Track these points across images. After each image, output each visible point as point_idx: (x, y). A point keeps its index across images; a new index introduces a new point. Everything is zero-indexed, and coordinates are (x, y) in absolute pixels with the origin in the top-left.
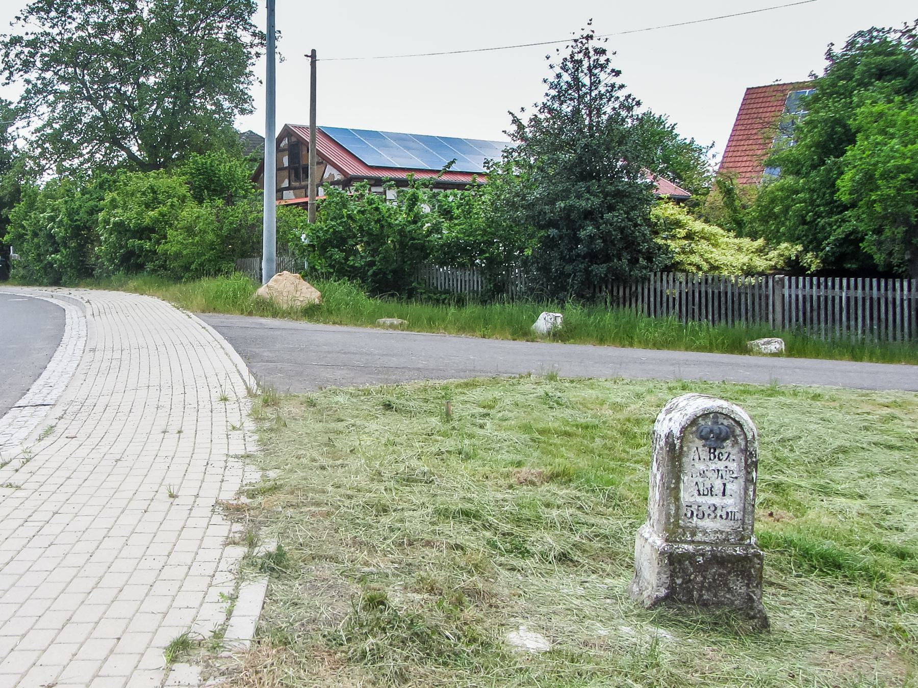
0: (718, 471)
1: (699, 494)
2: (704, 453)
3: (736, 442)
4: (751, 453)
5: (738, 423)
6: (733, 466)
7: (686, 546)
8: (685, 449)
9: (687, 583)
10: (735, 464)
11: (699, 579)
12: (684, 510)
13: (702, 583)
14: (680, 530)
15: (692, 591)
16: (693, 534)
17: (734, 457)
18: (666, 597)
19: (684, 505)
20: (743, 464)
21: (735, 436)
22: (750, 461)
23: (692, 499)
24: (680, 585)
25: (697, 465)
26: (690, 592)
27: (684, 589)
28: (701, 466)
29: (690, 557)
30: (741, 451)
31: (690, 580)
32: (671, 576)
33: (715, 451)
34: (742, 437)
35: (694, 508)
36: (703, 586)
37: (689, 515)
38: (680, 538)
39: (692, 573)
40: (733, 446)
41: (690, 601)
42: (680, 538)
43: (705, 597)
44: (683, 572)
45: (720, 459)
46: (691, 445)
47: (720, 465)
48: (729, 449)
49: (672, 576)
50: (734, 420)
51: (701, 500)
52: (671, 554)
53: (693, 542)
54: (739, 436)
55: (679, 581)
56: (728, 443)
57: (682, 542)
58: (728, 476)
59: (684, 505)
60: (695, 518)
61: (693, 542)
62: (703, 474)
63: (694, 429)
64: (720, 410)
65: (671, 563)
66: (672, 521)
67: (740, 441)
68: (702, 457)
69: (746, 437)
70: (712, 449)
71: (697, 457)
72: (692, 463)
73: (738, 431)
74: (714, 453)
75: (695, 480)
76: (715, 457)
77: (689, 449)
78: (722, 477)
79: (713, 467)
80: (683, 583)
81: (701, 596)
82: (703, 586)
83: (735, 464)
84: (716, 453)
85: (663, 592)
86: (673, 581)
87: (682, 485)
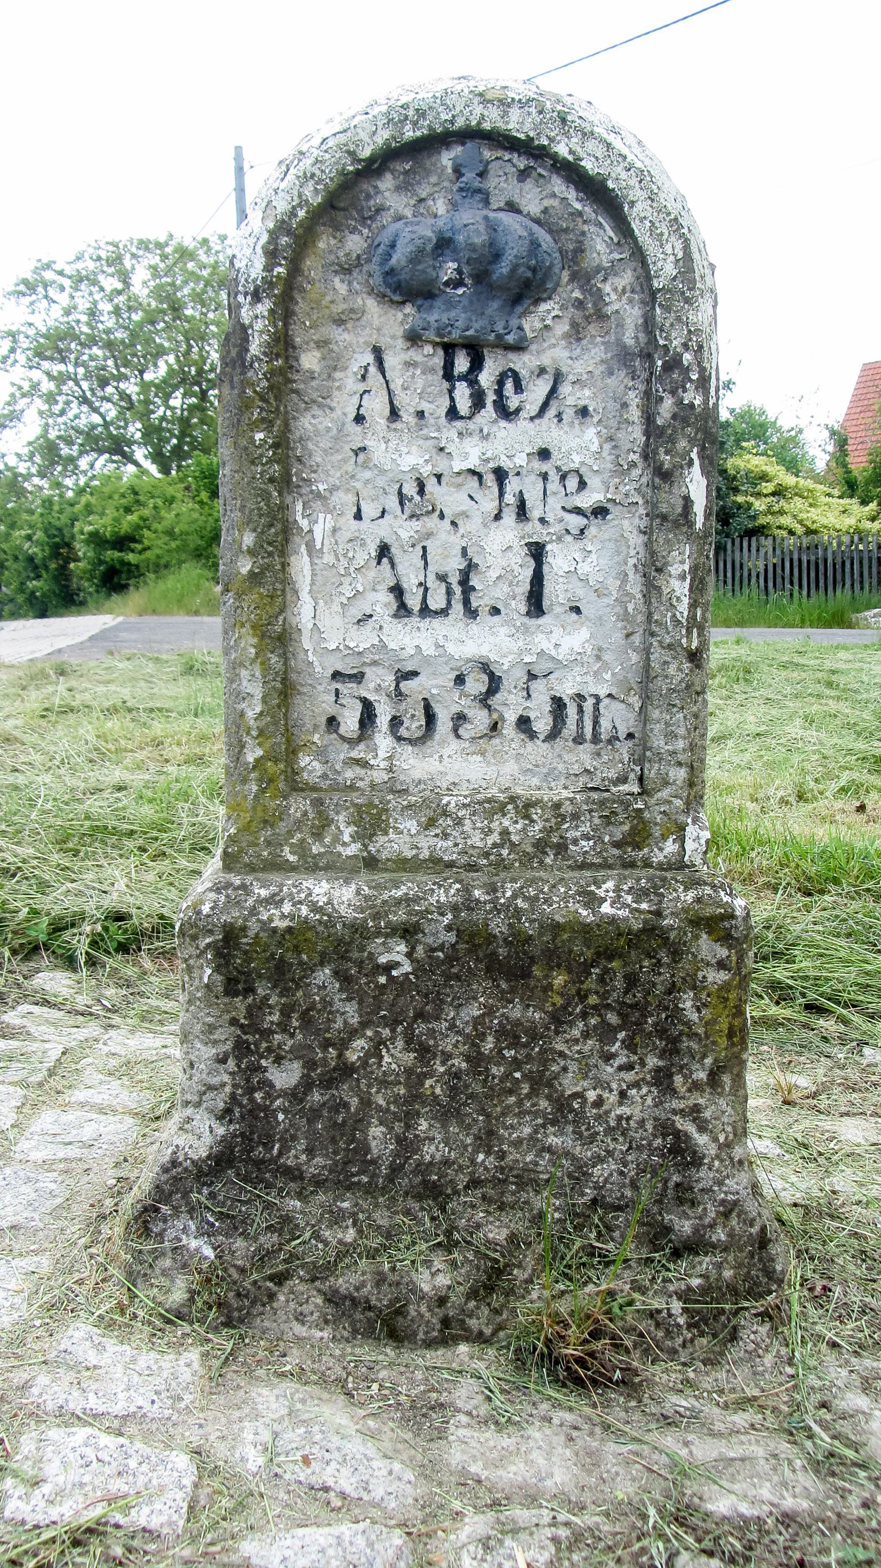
0: (500, 475)
1: (402, 610)
2: (416, 378)
3: (591, 314)
4: (673, 364)
5: (595, 190)
6: (579, 445)
7: (320, 889)
8: (309, 360)
9: (328, 1082)
10: (591, 435)
11: (396, 1058)
12: (317, 702)
13: (414, 1078)
14: (299, 806)
15: (360, 1122)
16: (372, 822)
17: (585, 396)
18: (221, 1161)
19: (322, 667)
20: (637, 434)
21: (583, 278)
22: (667, 407)
23: (363, 639)
24: (296, 1095)
25: (379, 452)
26: (347, 1130)
27: (314, 1114)
28: (409, 457)
29: (342, 946)
30: (624, 357)
31: (346, 1070)
32: (241, 1049)
33: (477, 364)
34: (626, 278)
35: (379, 680)
36: (415, 1096)
37: (350, 723)
38: (301, 849)
39: (353, 1033)
40: (576, 333)
41: (351, 1171)
42: (301, 849)
43: (430, 1152)
44: (307, 1021)
45: (505, 413)
46: (341, 336)
47: (508, 443)
48: (554, 353)
49: (247, 1050)
50: (571, 172)
51: (410, 639)
52: (231, 936)
53: (371, 863)
54: (610, 271)
55: (285, 1076)
56: (548, 315)
57: (312, 866)
58: (555, 503)
59: (322, 667)
60: (383, 741)
61: (371, 863)
62: (415, 497)
63: (355, 243)
64: (492, 119)
65: (236, 983)
66: (252, 755)
67: (614, 303)
68: (408, 403)
69: (645, 276)
70: (463, 353)
71: (376, 406)
72: (355, 435)
73: (601, 244)
74: (470, 377)
75: (374, 532)
76: (478, 401)
77: (334, 364)
78: (522, 511)
79: (470, 453)
80: (307, 1084)
81: (406, 1146)
82: (415, 1096)
83: (591, 435)
84: (486, 378)
85: (198, 1136)
86: (250, 1077)
87: (301, 566)
